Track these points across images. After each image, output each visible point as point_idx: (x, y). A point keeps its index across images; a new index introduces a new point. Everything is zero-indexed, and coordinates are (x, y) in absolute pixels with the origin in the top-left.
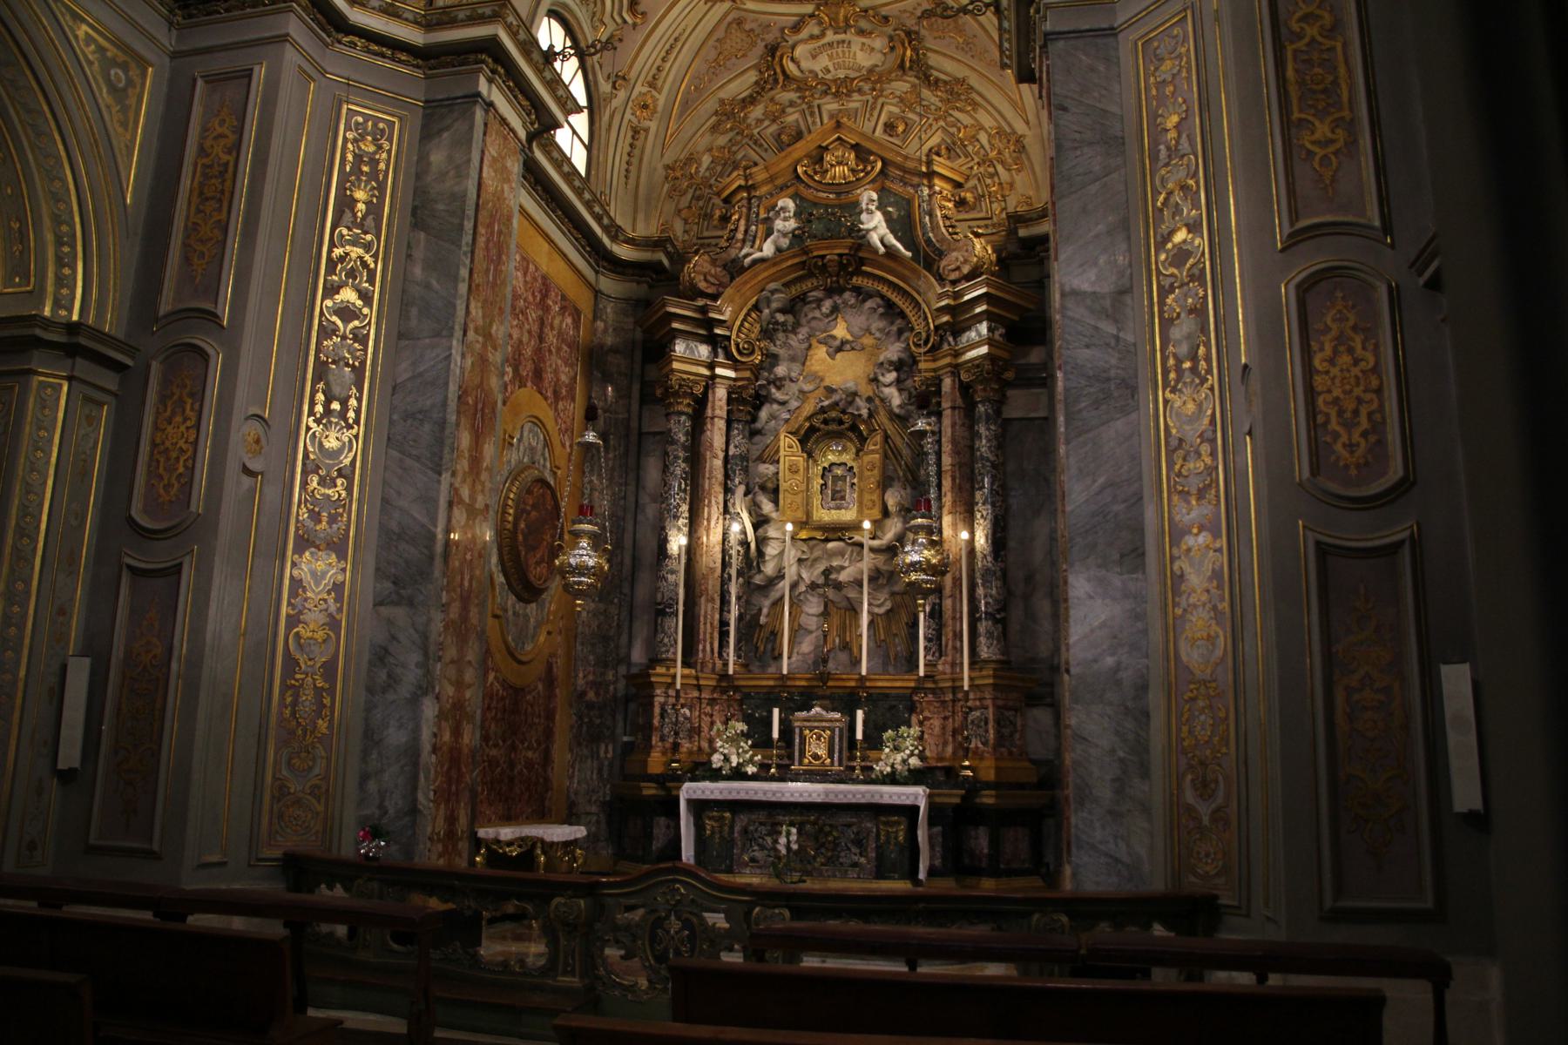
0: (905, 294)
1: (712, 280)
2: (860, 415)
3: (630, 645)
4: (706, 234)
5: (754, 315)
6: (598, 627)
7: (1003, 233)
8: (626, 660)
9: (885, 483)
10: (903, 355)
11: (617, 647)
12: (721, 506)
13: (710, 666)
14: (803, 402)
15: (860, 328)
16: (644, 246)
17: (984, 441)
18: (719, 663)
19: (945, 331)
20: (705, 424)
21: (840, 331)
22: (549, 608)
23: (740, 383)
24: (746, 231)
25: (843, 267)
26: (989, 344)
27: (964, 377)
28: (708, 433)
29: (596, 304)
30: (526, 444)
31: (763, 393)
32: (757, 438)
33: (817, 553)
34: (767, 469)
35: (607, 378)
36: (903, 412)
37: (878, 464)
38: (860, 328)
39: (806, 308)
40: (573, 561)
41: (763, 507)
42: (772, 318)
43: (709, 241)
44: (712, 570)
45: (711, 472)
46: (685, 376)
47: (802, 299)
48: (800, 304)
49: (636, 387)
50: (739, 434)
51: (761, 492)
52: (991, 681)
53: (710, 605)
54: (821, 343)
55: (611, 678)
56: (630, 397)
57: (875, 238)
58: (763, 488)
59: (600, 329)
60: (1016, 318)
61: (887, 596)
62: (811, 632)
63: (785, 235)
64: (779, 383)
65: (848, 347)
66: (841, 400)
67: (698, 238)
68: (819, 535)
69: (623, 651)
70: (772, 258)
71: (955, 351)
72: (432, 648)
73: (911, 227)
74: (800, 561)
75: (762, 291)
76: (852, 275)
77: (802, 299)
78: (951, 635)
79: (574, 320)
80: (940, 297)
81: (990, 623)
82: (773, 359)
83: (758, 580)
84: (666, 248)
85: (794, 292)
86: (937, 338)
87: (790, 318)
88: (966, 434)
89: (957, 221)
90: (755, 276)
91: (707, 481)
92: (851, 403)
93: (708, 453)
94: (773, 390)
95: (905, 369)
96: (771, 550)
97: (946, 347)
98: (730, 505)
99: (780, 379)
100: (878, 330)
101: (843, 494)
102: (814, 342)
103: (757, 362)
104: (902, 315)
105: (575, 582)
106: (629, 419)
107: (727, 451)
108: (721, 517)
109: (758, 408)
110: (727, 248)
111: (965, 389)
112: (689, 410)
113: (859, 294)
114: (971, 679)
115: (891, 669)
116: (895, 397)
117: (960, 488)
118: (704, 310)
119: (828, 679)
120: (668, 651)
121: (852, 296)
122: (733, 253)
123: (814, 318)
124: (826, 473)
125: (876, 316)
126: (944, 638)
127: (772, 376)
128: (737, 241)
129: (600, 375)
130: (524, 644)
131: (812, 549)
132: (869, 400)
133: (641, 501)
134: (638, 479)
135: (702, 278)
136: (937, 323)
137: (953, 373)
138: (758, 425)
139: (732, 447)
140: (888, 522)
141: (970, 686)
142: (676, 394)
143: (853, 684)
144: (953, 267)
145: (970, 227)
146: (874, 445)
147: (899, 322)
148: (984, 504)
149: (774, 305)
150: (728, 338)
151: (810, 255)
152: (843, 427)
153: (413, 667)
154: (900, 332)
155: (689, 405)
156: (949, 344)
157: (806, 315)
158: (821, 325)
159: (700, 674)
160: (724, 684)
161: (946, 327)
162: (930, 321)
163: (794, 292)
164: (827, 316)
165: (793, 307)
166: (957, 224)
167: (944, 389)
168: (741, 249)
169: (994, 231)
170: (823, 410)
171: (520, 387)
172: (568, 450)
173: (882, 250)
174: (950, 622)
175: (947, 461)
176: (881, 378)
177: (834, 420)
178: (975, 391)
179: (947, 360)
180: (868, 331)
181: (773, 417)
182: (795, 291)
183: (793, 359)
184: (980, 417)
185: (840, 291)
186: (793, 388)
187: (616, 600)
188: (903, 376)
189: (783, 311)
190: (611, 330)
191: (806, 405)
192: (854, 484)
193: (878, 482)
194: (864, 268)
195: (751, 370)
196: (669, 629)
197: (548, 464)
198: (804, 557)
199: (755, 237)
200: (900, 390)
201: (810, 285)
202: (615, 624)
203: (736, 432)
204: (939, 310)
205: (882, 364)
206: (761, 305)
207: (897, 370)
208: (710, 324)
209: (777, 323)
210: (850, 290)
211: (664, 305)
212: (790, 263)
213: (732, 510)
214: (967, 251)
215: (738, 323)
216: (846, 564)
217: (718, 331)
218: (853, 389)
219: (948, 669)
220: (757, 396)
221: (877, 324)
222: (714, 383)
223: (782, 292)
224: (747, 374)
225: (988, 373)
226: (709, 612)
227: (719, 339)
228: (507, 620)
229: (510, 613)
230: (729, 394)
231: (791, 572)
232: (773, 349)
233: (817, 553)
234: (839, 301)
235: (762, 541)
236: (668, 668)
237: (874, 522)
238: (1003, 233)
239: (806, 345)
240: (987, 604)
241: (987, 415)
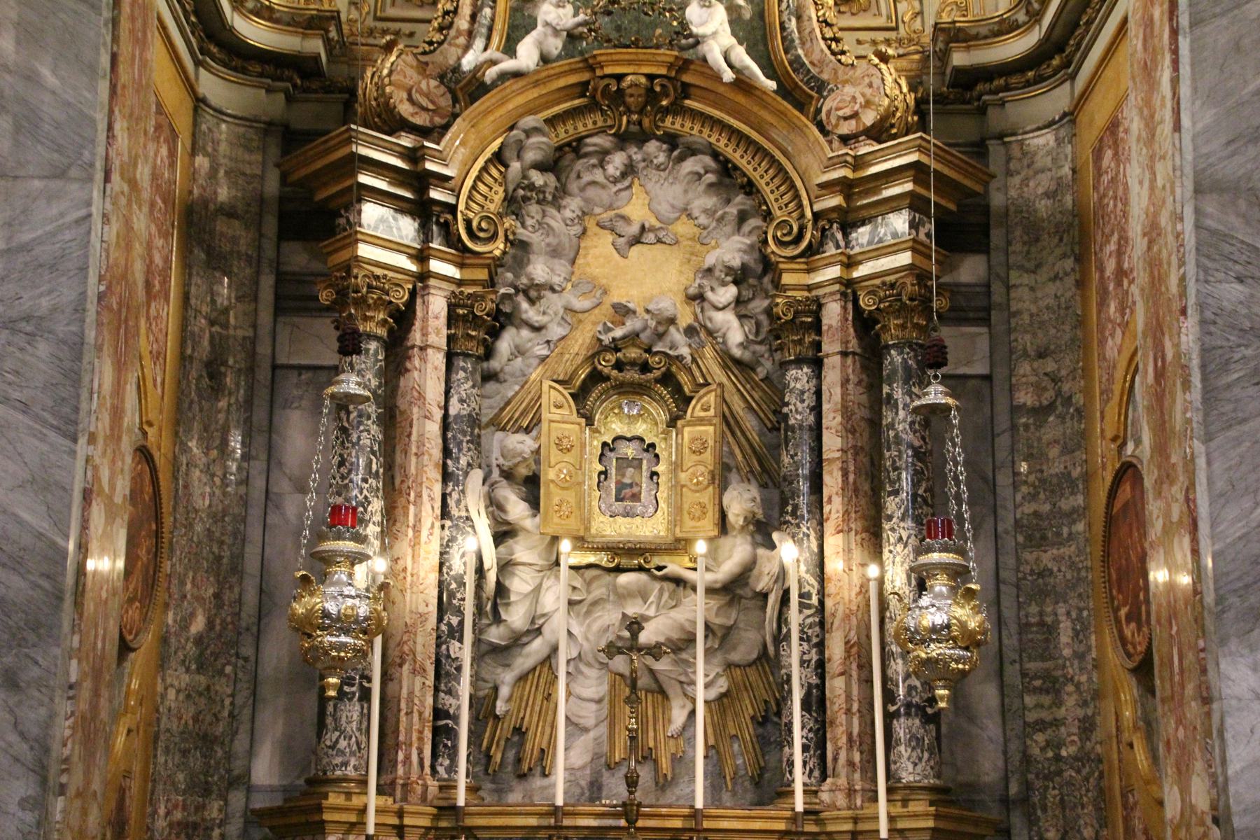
0: (758, 150)
1: (425, 102)
2: (680, 358)
3: (251, 753)
4: (391, 12)
5: (494, 172)
6: (196, 719)
7: (917, 57)
8: (242, 781)
9: (721, 478)
10: (746, 258)
11: (229, 756)
12: (438, 504)
13: (419, 789)
14: (573, 328)
15: (673, 206)
16: (289, 24)
17: (902, 414)
18: (433, 785)
19: (831, 222)
20: (409, 358)
21: (637, 210)
22: (129, 686)
23: (469, 290)
24: (473, 17)
25: (651, 96)
26: (913, 250)
27: (867, 303)
28: (416, 374)
29: (195, 124)
31: (507, 308)
32: (491, 387)
33: (598, 591)
34: (521, 443)
35: (217, 262)
36: (746, 356)
37: (711, 443)
38: (673, 206)
39: (580, 165)
40: (332, 607)
41: (509, 507)
42: (525, 177)
43: (396, 26)
44: (423, 617)
45: (421, 444)
46: (379, 272)
47: (575, 147)
48: (570, 156)
49: (267, 283)
50: (467, 379)
51: (504, 482)
52: (930, 823)
53: (418, 681)
54: (603, 227)
55: (215, 814)
56: (256, 299)
57: (714, 52)
58: (508, 475)
59: (203, 172)
60: (952, 207)
61: (719, 670)
62: (585, 730)
63: (556, 32)
64: (534, 292)
65: (650, 237)
66: (645, 328)
67: (377, 19)
68: (603, 559)
69: (238, 767)
70: (536, 72)
71: (849, 257)
72: (54, 769)
73: (764, 37)
74: (571, 603)
75: (512, 128)
76: (666, 111)
77: (575, 147)
78: (844, 739)
79: (169, 149)
80: (831, 164)
81: (917, 722)
82: (521, 247)
83: (495, 635)
84: (327, 31)
85: (563, 135)
86: (818, 234)
87: (551, 179)
88: (864, 398)
89: (841, 29)
90: (503, 101)
91: (413, 459)
92: (660, 336)
93: (415, 410)
94: (525, 305)
95: (752, 281)
96: (519, 584)
97: (831, 250)
98: (451, 502)
99: (539, 287)
100: (705, 211)
101: (635, 490)
102: (590, 224)
103: (497, 253)
104: (750, 188)
105: (333, 646)
106: (254, 341)
107: (446, 408)
108: (438, 524)
109: (495, 333)
110: (440, 43)
111: (865, 324)
112: (382, 332)
113: (673, 147)
114: (891, 819)
115: (726, 797)
116: (735, 333)
117: (856, 490)
118: (415, 156)
119: (639, 815)
120: (346, 764)
121: (660, 149)
122: (449, 54)
123: (593, 183)
124: (609, 454)
125: (702, 188)
126: (829, 746)
127: (524, 280)
128: (459, 33)
129: (203, 256)
131: (589, 584)
132: (690, 331)
133: (274, 489)
134: (270, 449)
135: (405, 96)
136: (817, 208)
137: (844, 295)
138: (495, 364)
139: (454, 401)
140: (726, 542)
141: (890, 830)
142: (361, 302)
143: (678, 824)
144: (847, 112)
145: (874, 42)
146: (704, 406)
147: (740, 200)
148: (903, 519)
149: (531, 156)
150: (452, 209)
151: (599, 73)
152: (650, 376)
153: (13, 808)
154: (742, 217)
155: (384, 323)
156: (838, 247)
157: (579, 177)
158: (604, 196)
159: (407, 807)
160: (443, 824)
161: (834, 215)
162: (806, 202)
163: (563, 135)
164: (615, 181)
165: (556, 161)
166: (839, 35)
167: (825, 321)
168: (467, 48)
169: (901, 51)
170: (615, 346)
172: (159, 390)
173: (728, 76)
174: (842, 718)
175: (832, 443)
176: (709, 295)
177: (633, 363)
178: (885, 328)
179: (834, 272)
180: (686, 212)
181: (519, 351)
182: (564, 133)
183: (555, 253)
184: (894, 372)
185: (641, 138)
186: (554, 303)
188: (747, 294)
189: (541, 167)
190: (221, 173)
191: (577, 334)
192: (656, 474)
193: (712, 474)
194: (688, 102)
195: (488, 266)
196: (349, 722)
198: (576, 598)
199: (490, 29)
200: (741, 317)
201: (590, 126)
202: (226, 713)
203: (462, 374)
204: (822, 186)
205: (710, 271)
206: (509, 154)
207: (736, 282)
208: (419, 180)
209: (531, 187)
210: (658, 139)
211: (349, 141)
212: (562, 82)
213: (454, 512)
214: (870, 85)
215: (469, 183)
216: (651, 612)
217: (435, 194)
218: (668, 314)
219: (841, 800)
220: (497, 314)
221: (703, 202)
222: (426, 287)
223: (544, 135)
224: (482, 275)
225: (911, 299)
226: (417, 693)
227: (436, 209)
230: (451, 307)
231: (558, 625)
232: (523, 234)
233: (598, 591)
234: (637, 157)
235: (505, 566)
236: (349, 795)
237: (711, 540)
238: (917, 57)
239: (577, 229)
240: (911, 689)
241: (907, 368)
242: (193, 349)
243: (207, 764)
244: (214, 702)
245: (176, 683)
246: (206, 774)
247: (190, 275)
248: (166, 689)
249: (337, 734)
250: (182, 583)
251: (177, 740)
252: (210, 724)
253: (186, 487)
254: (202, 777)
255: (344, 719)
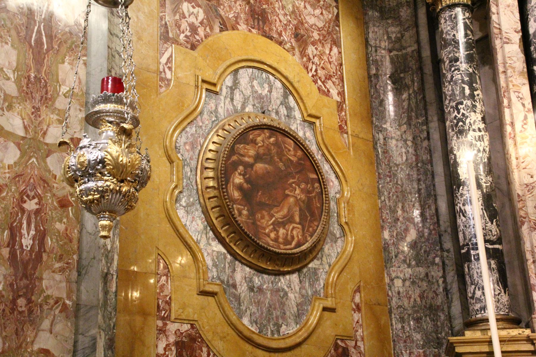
6: (421, 297)
30: (248, 92)
45: (505, 63)
106: (419, 51)
130: (279, 326)
171: (221, 30)
187: (437, 260)
197: (297, 114)
202: (441, 290)
228: (238, 298)
229: (243, 289)
242: (377, 69)
243: (436, 325)
244: (433, 283)
245: (402, 276)
246: (436, 332)
247: (368, 28)
248: (392, 280)
249: (473, 287)
250: (393, 211)
251: (410, 312)
252: (432, 298)
253: (385, 152)
254: (434, 334)
255: (475, 275)
